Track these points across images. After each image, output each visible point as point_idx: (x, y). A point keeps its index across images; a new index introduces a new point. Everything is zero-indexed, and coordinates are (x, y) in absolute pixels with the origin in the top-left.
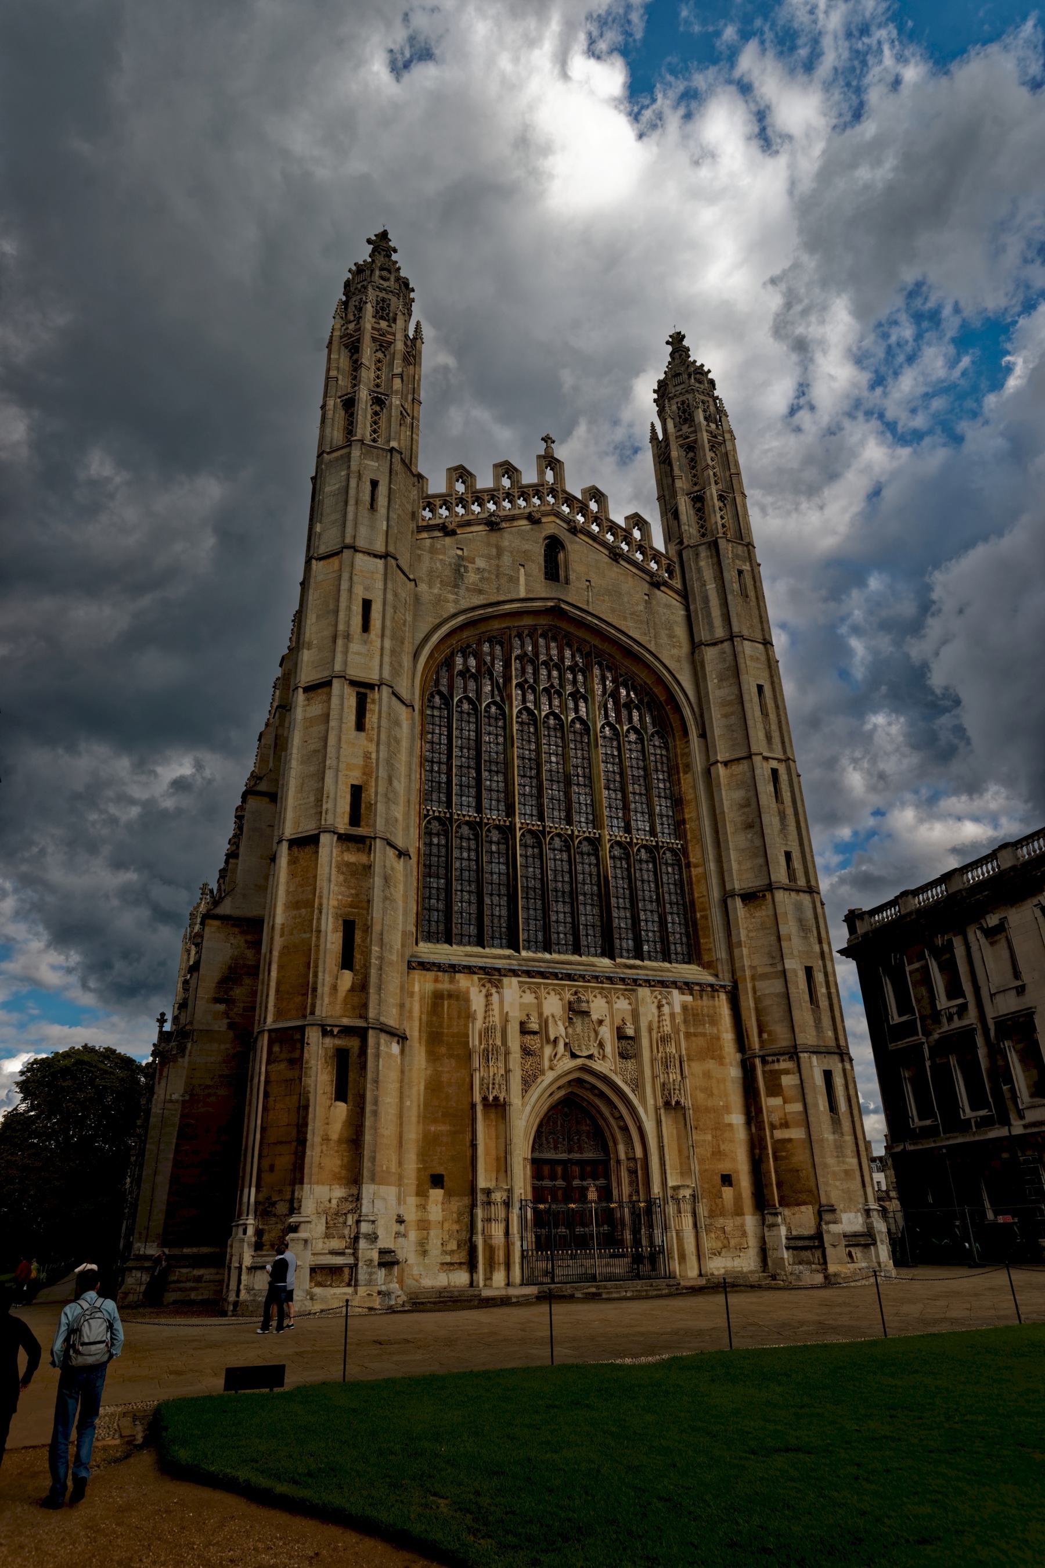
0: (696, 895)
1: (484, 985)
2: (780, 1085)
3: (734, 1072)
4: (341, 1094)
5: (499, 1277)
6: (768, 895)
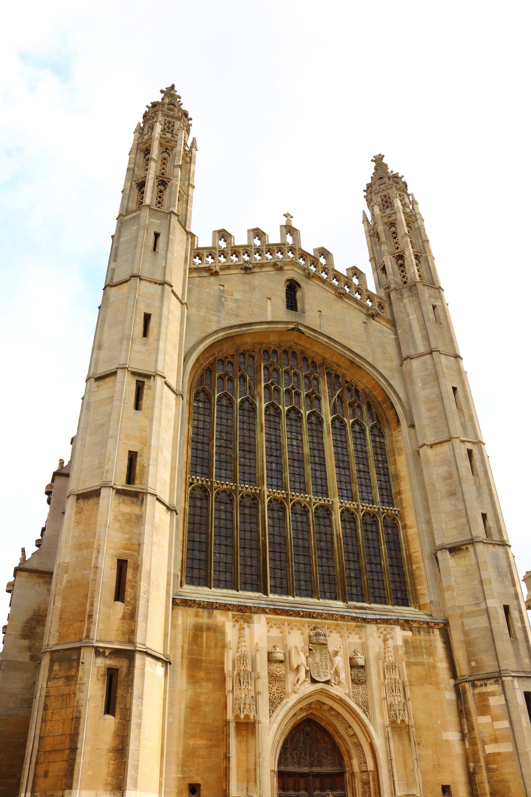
0: (412, 551)
1: (237, 621)
2: (488, 706)
3: (450, 696)
4: (109, 709)
6: (470, 547)
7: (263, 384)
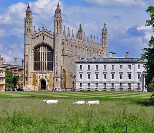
5: (37, 90)
7: (40, 50)
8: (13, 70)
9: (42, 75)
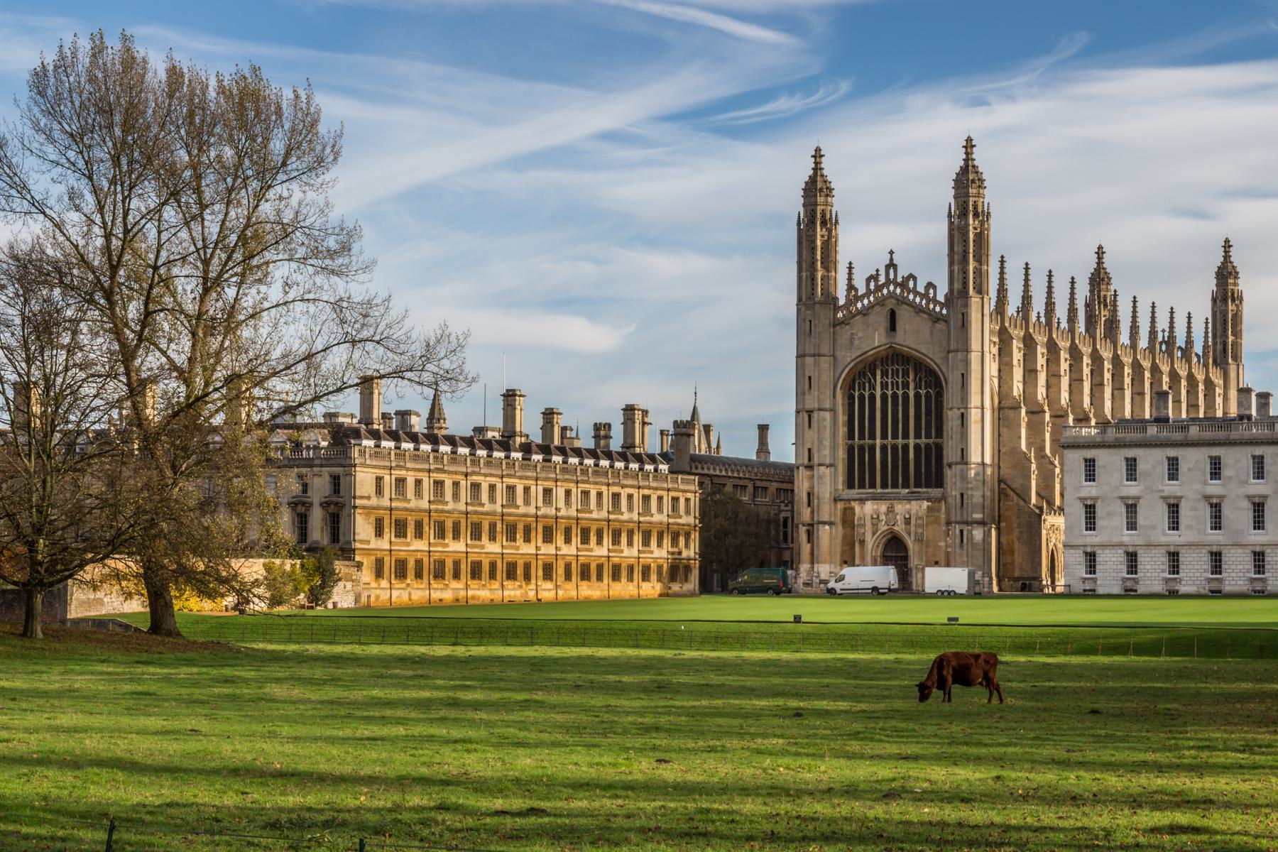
3: (944, 528)
8: (750, 487)
9: (890, 510)
